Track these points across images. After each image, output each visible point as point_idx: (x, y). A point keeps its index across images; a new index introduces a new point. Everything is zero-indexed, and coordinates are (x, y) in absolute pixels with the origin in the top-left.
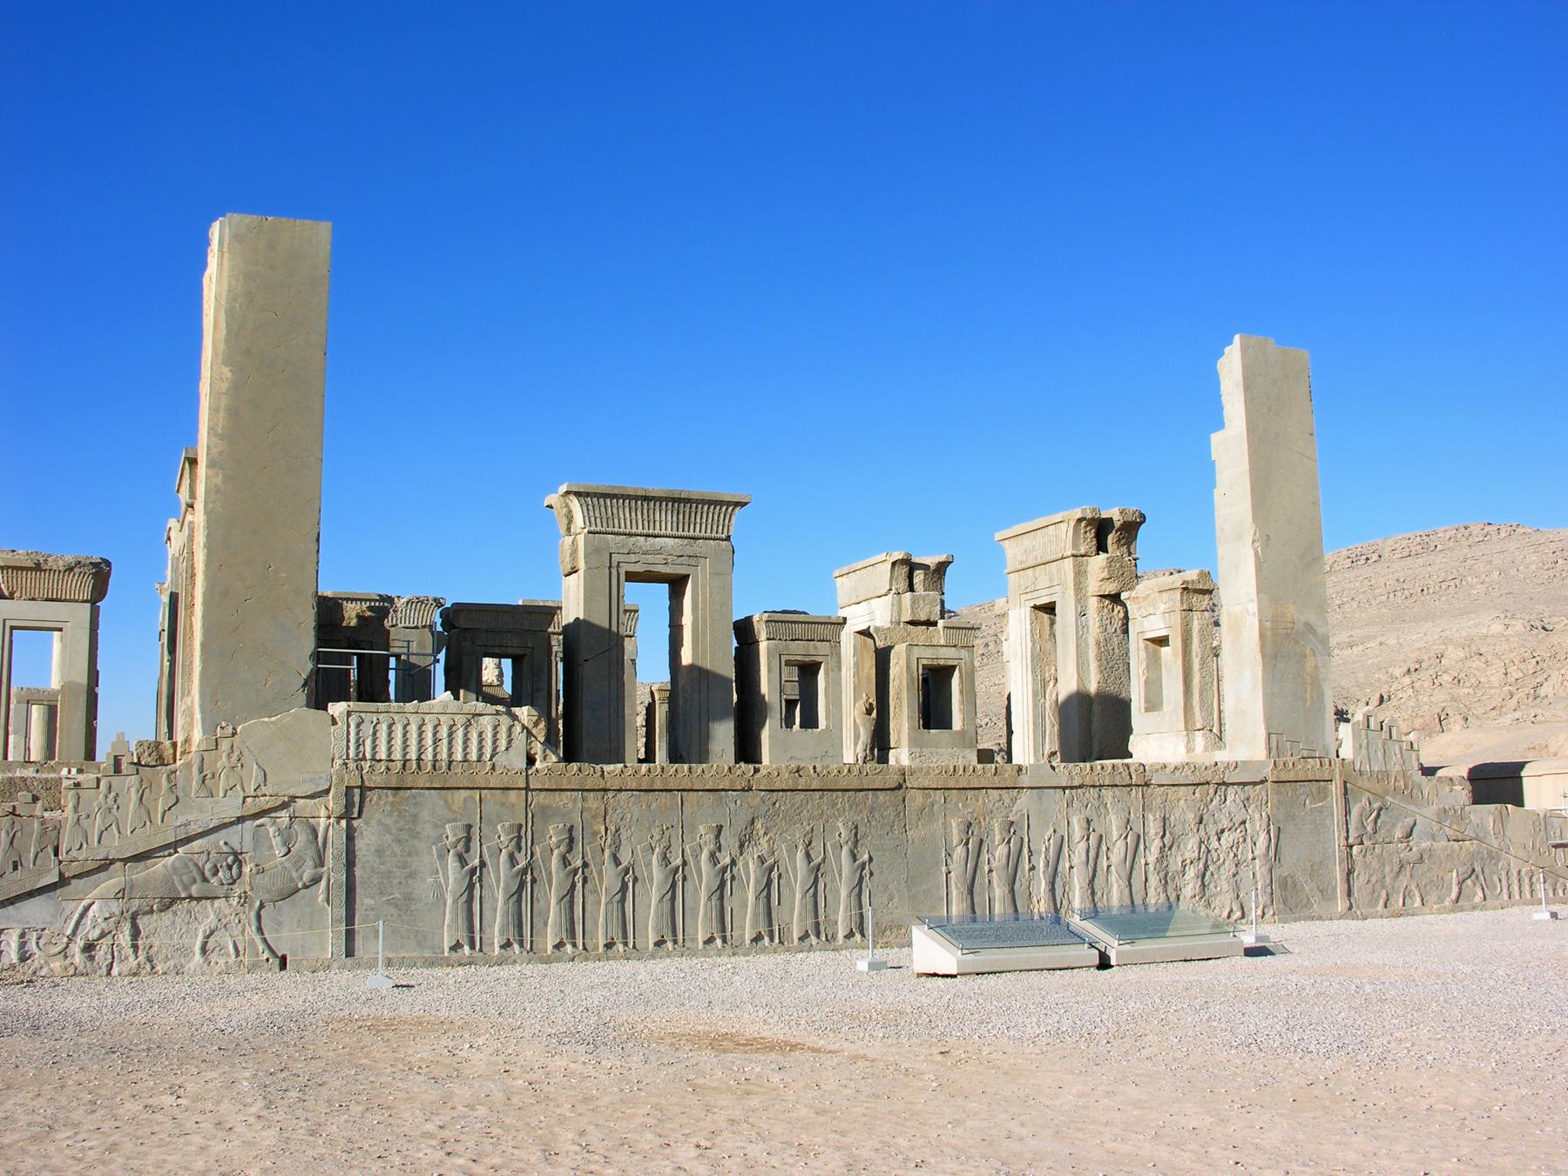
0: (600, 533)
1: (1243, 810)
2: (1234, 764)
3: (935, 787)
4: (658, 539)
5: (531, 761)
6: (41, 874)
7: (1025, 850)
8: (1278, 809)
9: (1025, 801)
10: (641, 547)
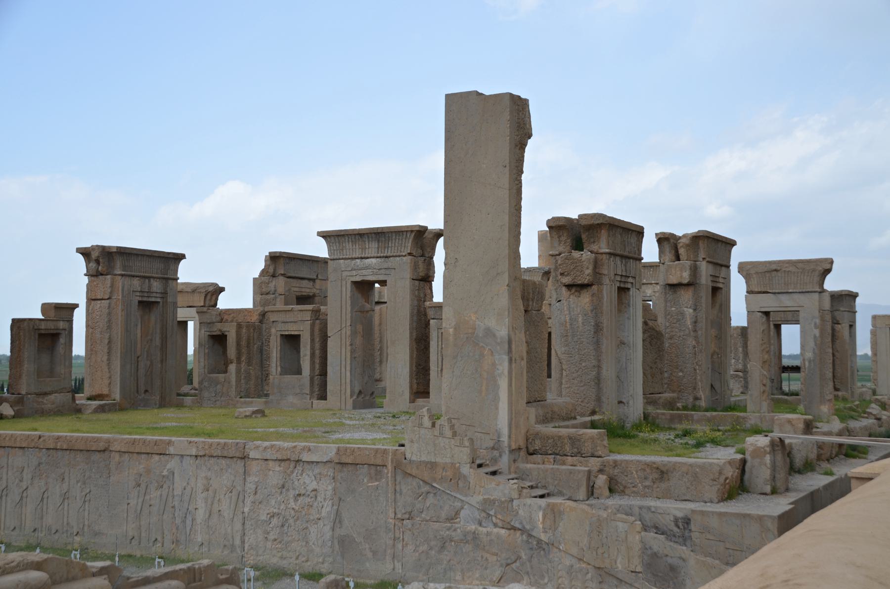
0: (337, 259)
1: (315, 483)
2: (307, 449)
4: (368, 260)
7: (171, 493)
9: (173, 464)
10: (358, 266)
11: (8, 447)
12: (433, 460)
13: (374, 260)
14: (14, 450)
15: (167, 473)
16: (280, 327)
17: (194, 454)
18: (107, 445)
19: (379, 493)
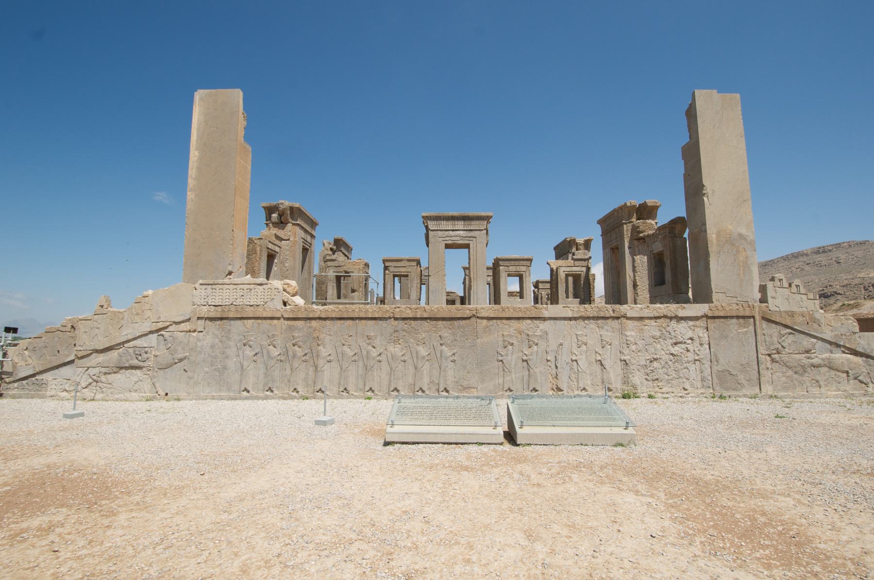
1: (690, 332)
3: (492, 316)
5: (285, 304)
6: (67, 356)
8: (714, 332)
11: (356, 318)
12: (788, 309)
13: (462, 232)
14: (363, 322)
15: (540, 333)
16: (392, 269)
17: (570, 316)
18: (474, 312)
19: (749, 337)
